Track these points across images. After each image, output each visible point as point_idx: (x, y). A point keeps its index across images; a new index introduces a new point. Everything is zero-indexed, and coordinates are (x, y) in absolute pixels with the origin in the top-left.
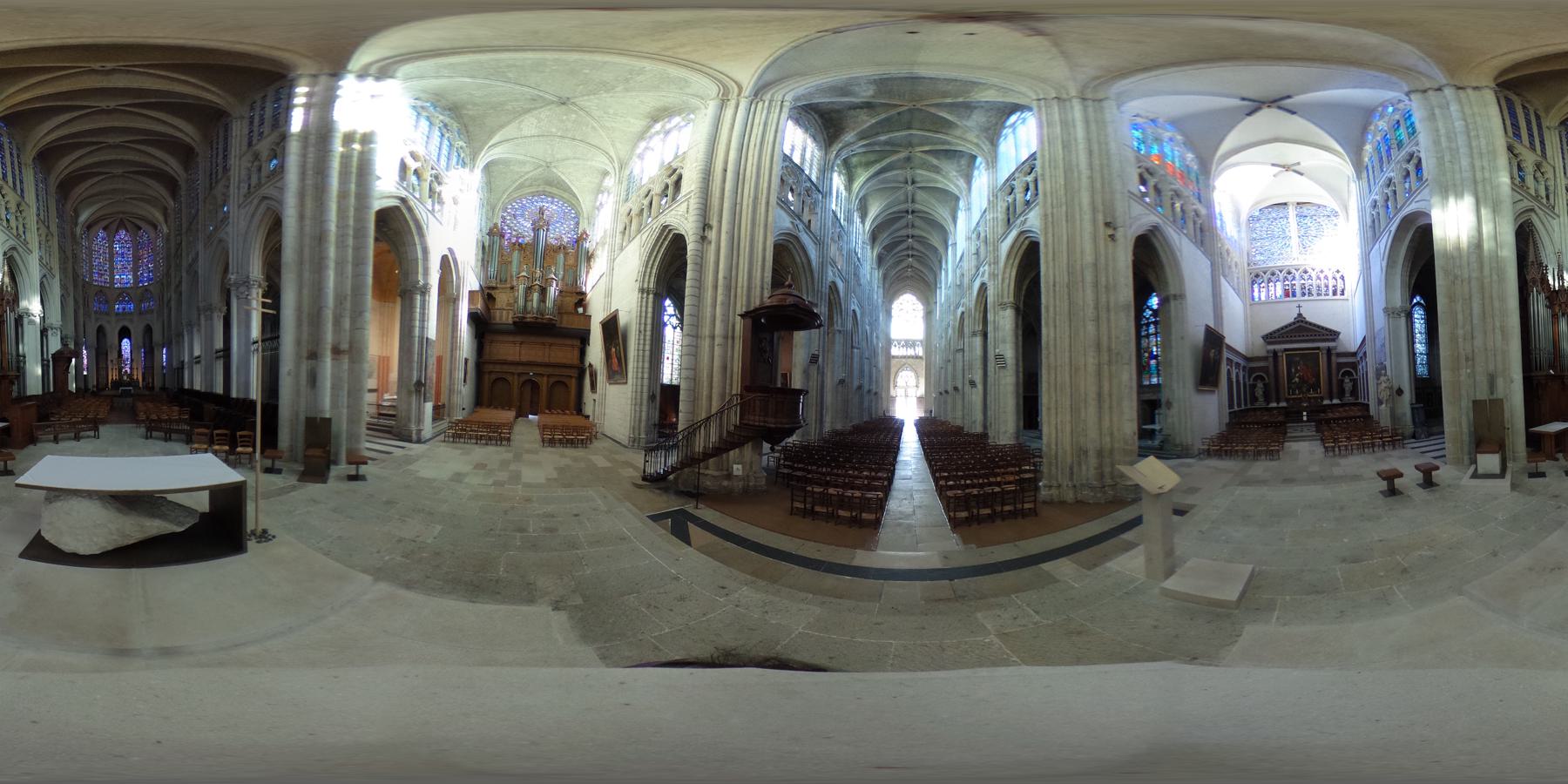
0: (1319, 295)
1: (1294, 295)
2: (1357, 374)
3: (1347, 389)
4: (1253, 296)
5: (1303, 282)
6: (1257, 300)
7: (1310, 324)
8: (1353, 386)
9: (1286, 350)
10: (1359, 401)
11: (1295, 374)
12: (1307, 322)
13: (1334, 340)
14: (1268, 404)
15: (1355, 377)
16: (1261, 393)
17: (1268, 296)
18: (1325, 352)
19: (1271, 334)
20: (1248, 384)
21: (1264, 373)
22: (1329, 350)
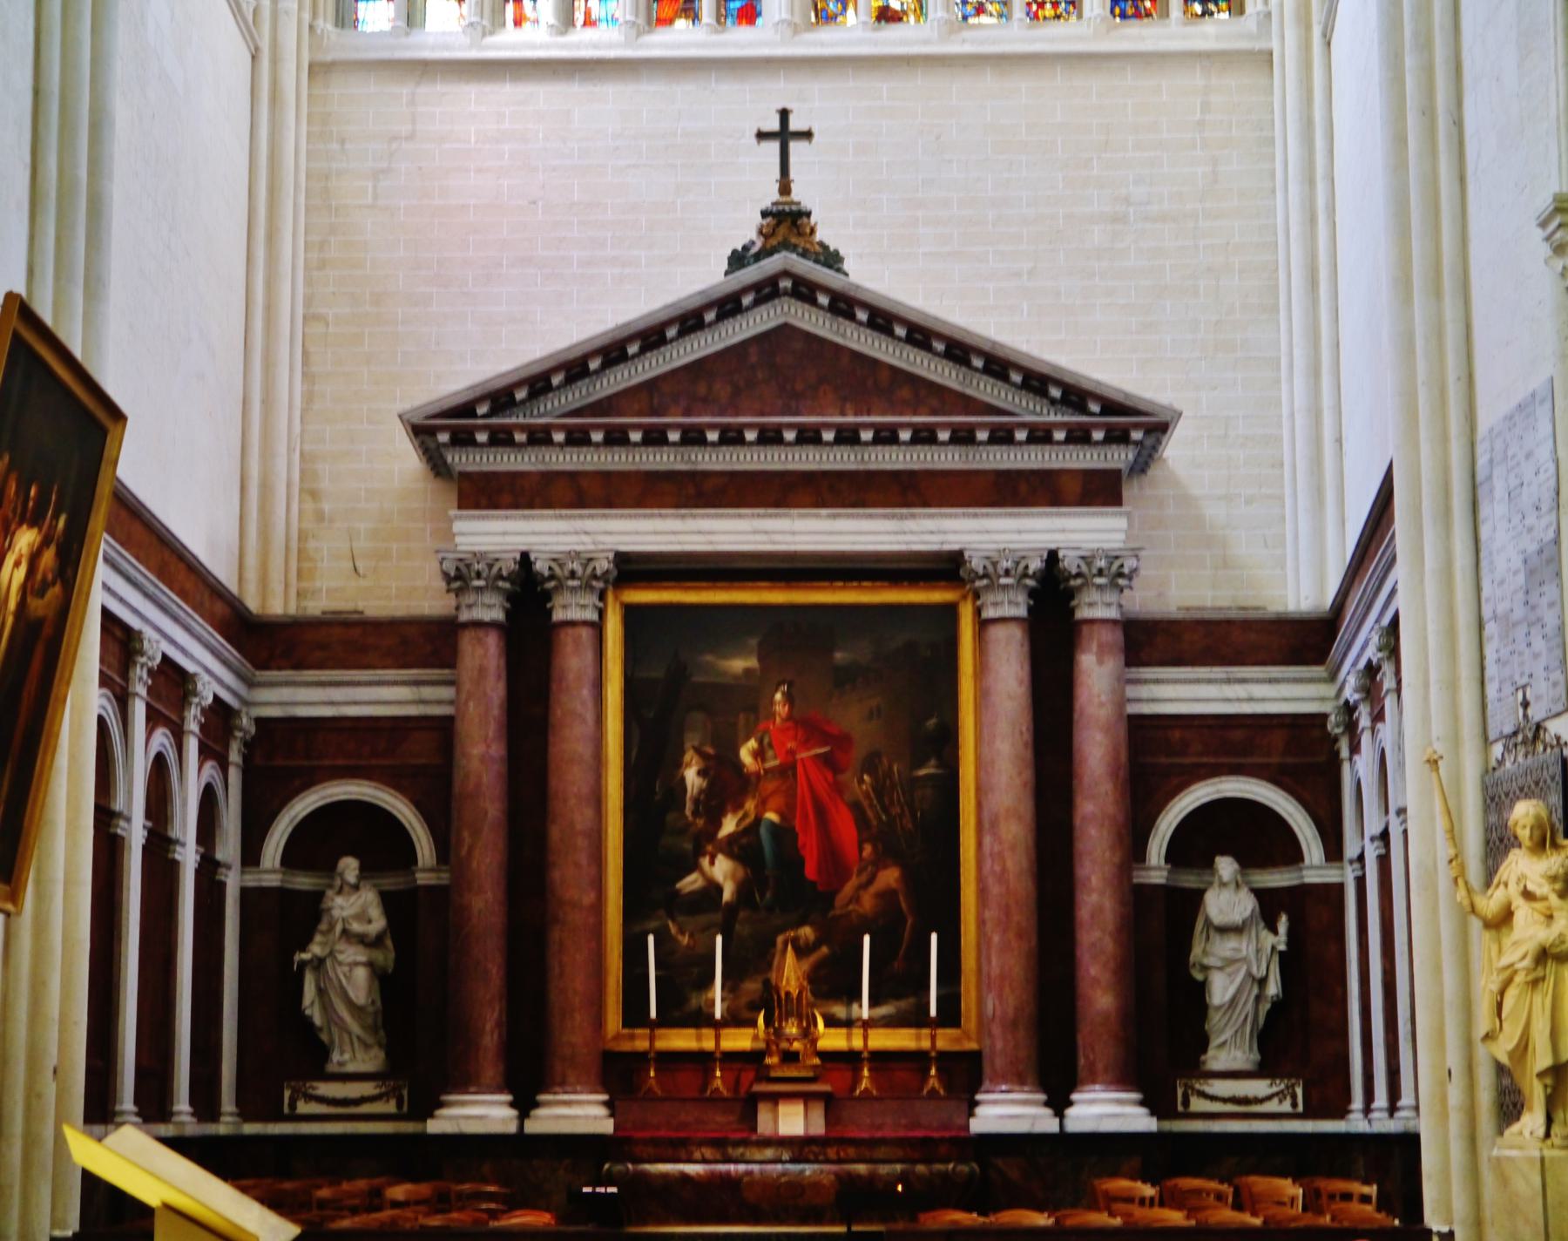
2: (1334, 851)
3: (1221, 989)
7: (882, 320)
8: (1289, 962)
10: (1355, 1123)
11: (714, 807)
12: (844, 305)
14: (426, 1106)
15: (1315, 868)
16: (359, 985)
18: (1011, 605)
19: (500, 398)
20: (233, 882)
21: (392, 779)
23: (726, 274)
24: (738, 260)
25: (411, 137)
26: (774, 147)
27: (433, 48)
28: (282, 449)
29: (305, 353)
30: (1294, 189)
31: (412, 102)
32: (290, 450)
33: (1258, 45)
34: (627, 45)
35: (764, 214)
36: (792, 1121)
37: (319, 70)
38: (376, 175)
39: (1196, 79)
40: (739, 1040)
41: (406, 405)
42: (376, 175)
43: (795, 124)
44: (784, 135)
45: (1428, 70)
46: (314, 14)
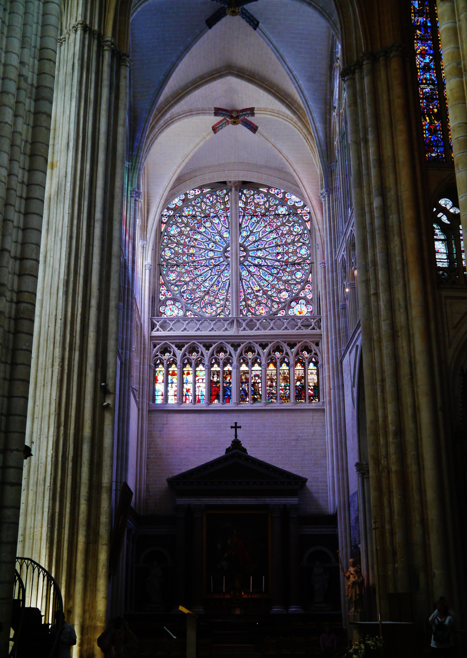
0: (271, 395)
1: (227, 398)
4: (154, 390)
5: (244, 368)
6: (159, 400)
7: (255, 461)
9: (208, 507)
13: (293, 493)
17: (181, 396)
22: (285, 509)
23: (226, 453)
24: (228, 450)
25: (167, 424)
26: (234, 429)
27: (171, 407)
28: (143, 483)
29: (147, 465)
30: (329, 435)
31: (167, 417)
32: (144, 483)
33: (322, 408)
34: (207, 407)
35: (232, 442)
36: (238, 612)
37: (150, 411)
38: (160, 431)
39: (311, 414)
40: (228, 596)
41: (167, 477)
42: (160, 431)
43: (238, 425)
44: (236, 427)
45: (341, 435)
46: (149, 401)
